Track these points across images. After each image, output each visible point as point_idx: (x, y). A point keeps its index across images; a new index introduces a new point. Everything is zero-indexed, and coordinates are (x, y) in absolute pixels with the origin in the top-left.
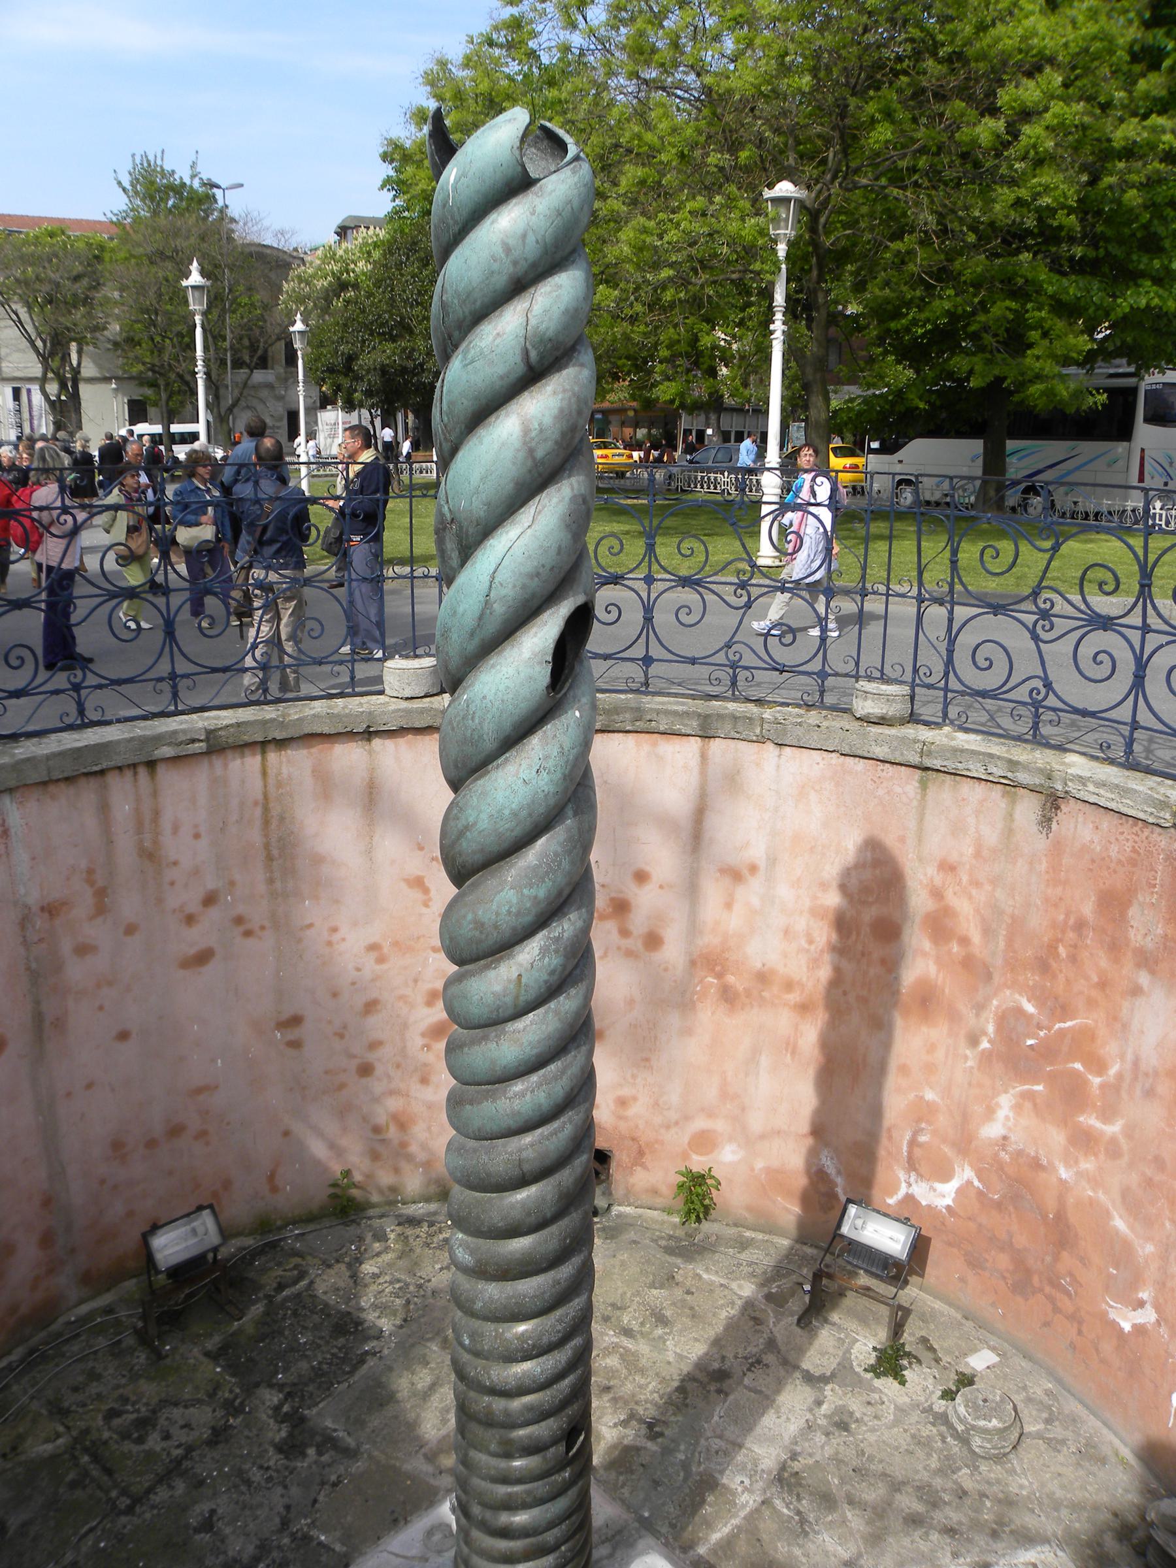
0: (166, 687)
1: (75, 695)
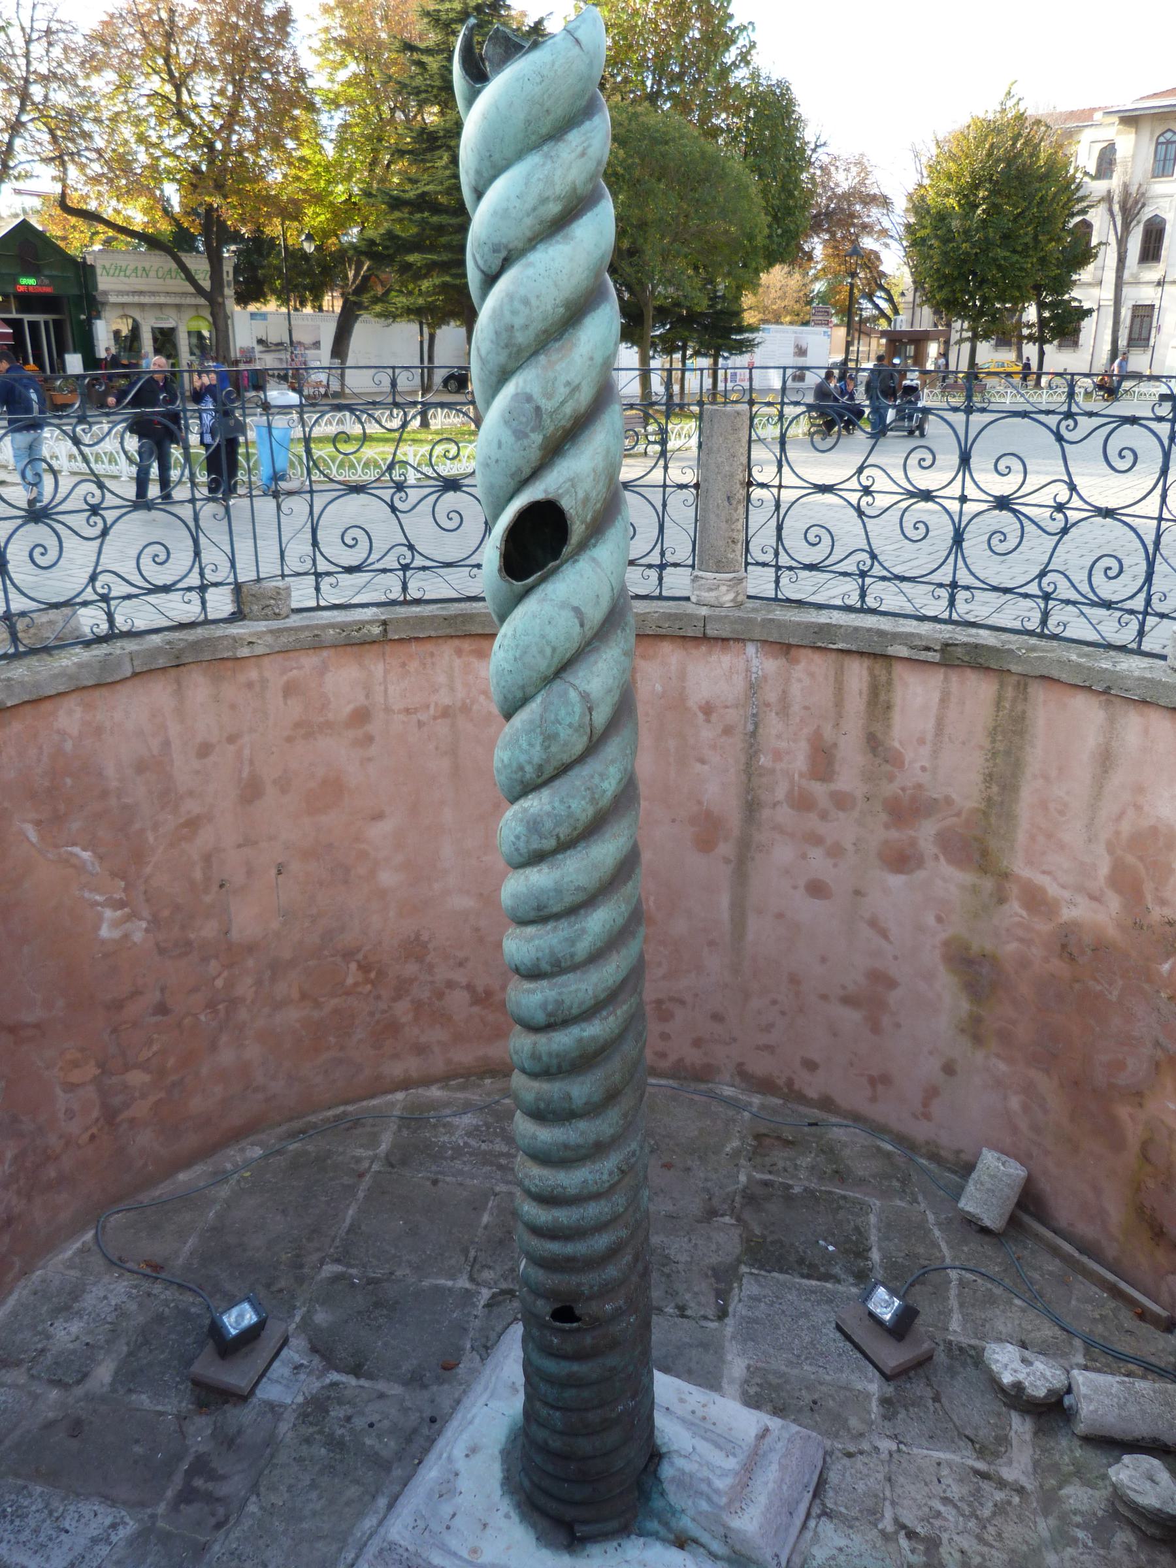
0: (944, 593)
1: (860, 581)
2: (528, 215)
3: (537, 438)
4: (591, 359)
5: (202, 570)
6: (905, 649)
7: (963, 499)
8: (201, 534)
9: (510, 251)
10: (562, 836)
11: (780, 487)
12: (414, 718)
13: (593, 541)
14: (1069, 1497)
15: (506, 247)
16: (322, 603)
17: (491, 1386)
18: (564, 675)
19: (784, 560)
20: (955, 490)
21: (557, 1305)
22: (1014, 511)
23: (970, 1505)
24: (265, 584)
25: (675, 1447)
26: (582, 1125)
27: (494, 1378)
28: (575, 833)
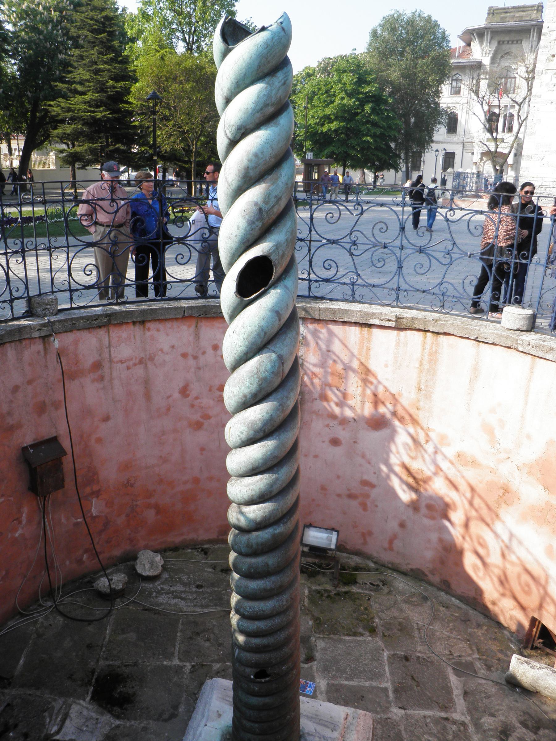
1: (351, 287)
2: (258, 112)
3: (259, 224)
4: (287, 184)
5: (11, 291)
6: (378, 320)
7: (402, 248)
8: (10, 272)
9: (246, 129)
10: (266, 430)
11: (310, 241)
12: (125, 365)
13: (284, 276)
14: (485, 723)
15: (244, 127)
16: (74, 306)
17: (206, 715)
18: (269, 346)
19: (313, 276)
20: (398, 243)
21: (258, 670)
22: (426, 254)
23: (443, 734)
24: (44, 297)
25: (306, 731)
26: (273, 578)
27: (206, 710)
28: (274, 428)
